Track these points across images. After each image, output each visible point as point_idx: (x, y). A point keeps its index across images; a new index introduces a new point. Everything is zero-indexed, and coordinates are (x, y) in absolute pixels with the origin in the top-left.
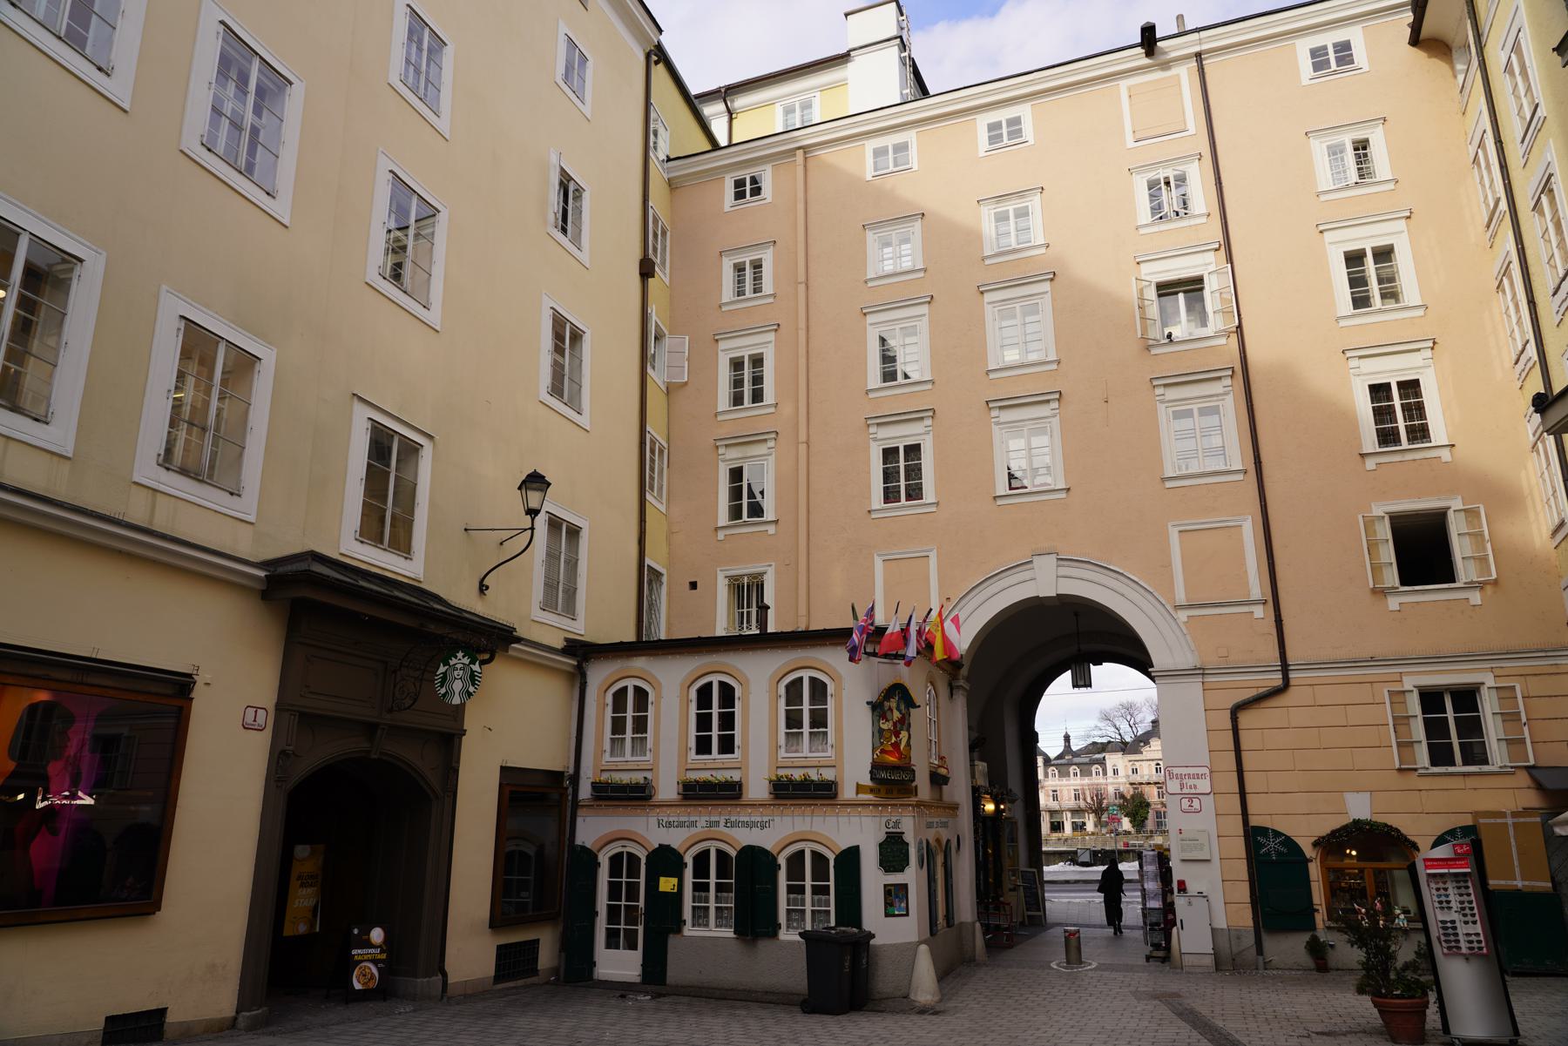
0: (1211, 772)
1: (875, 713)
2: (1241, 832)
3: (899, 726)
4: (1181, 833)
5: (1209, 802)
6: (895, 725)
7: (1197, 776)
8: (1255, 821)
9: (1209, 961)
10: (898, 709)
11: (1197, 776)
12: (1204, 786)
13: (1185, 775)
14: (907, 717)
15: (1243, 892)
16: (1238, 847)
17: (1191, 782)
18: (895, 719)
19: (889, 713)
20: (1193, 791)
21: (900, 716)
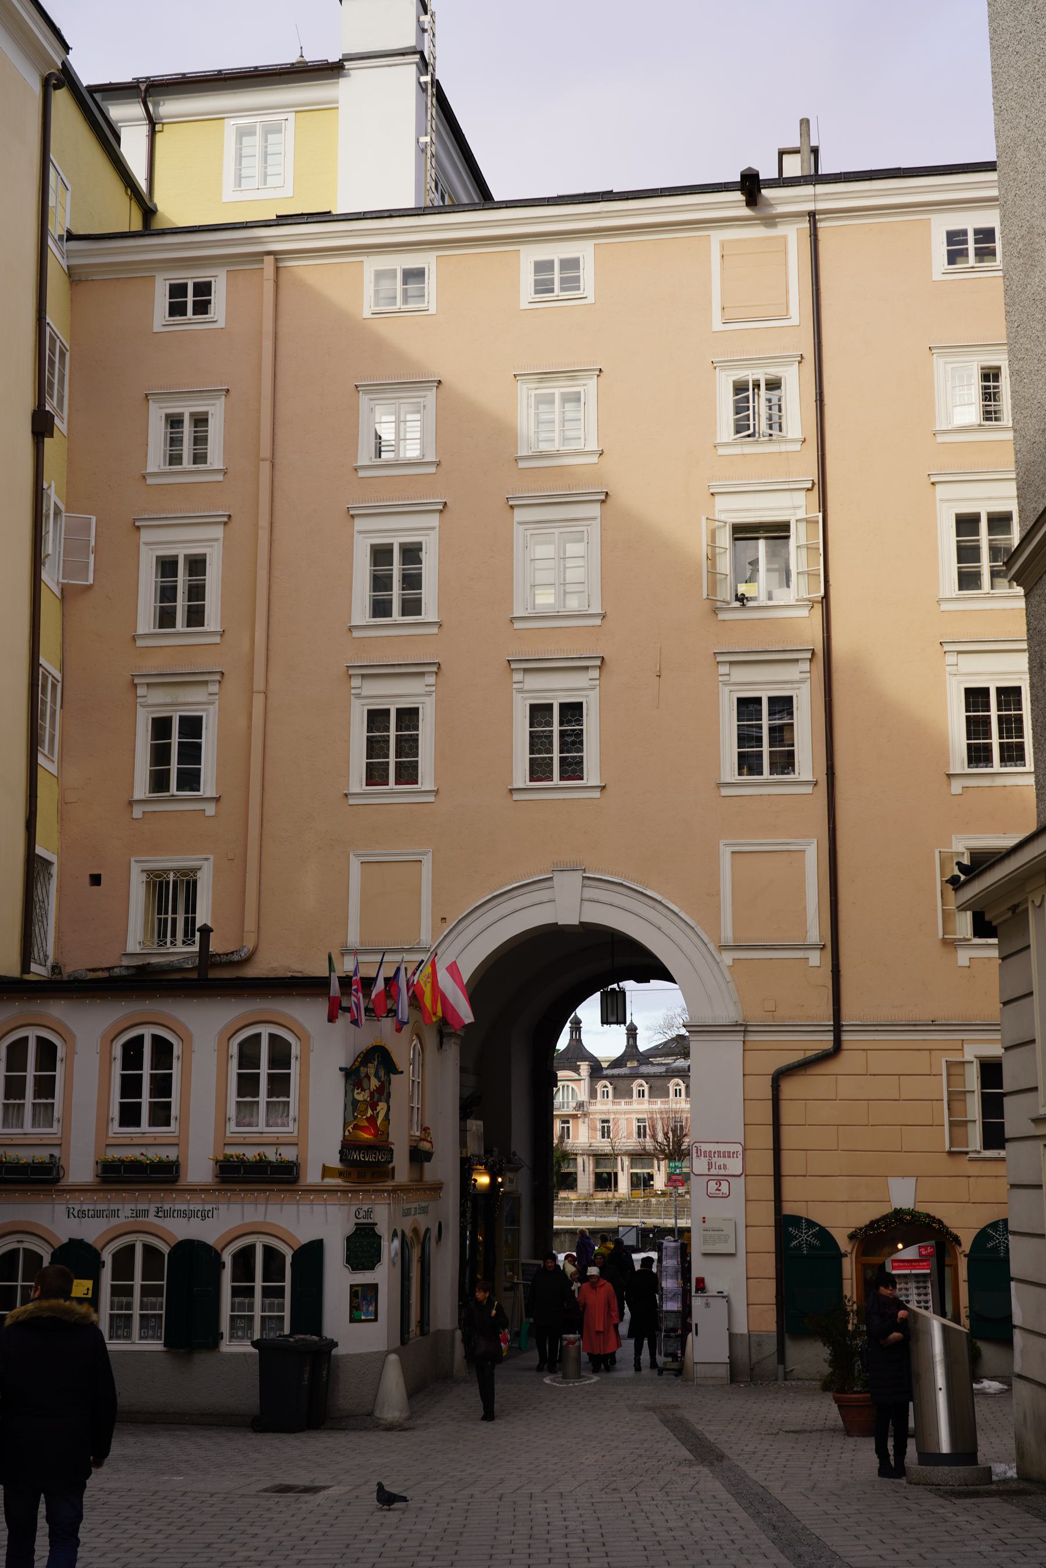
0: (744, 1150)
1: (350, 1081)
2: (771, 1220)
3: (376, 1096)
4: (704, 1222)
5: (738, 1184)
6: (372, 1095)
7: (729, 1155)
8: (789, 1209)
9: (724, 1371)
10: (377, 1076)
11: (729, 1155)
12: (735, 1166)
13: (715, 1152)
14: (387, 1084)
15: (768, 1291)
16: (767, 1238)
17: (721, 1161)
18: (373, 1087)
19: (365, 1082)
20: (722, 1172)
21: (378, 1084)
